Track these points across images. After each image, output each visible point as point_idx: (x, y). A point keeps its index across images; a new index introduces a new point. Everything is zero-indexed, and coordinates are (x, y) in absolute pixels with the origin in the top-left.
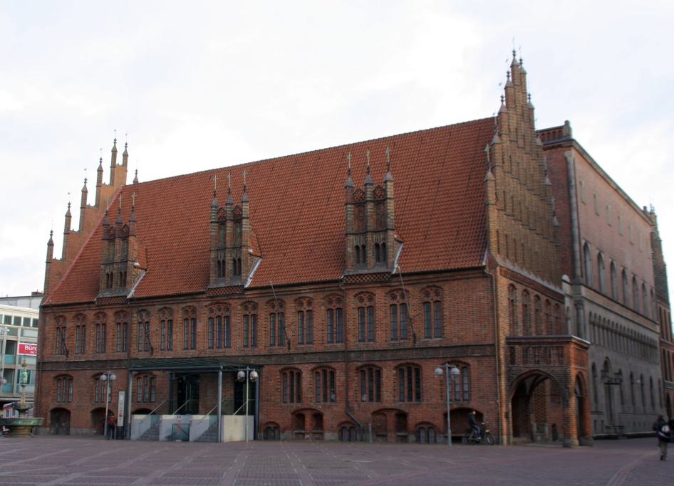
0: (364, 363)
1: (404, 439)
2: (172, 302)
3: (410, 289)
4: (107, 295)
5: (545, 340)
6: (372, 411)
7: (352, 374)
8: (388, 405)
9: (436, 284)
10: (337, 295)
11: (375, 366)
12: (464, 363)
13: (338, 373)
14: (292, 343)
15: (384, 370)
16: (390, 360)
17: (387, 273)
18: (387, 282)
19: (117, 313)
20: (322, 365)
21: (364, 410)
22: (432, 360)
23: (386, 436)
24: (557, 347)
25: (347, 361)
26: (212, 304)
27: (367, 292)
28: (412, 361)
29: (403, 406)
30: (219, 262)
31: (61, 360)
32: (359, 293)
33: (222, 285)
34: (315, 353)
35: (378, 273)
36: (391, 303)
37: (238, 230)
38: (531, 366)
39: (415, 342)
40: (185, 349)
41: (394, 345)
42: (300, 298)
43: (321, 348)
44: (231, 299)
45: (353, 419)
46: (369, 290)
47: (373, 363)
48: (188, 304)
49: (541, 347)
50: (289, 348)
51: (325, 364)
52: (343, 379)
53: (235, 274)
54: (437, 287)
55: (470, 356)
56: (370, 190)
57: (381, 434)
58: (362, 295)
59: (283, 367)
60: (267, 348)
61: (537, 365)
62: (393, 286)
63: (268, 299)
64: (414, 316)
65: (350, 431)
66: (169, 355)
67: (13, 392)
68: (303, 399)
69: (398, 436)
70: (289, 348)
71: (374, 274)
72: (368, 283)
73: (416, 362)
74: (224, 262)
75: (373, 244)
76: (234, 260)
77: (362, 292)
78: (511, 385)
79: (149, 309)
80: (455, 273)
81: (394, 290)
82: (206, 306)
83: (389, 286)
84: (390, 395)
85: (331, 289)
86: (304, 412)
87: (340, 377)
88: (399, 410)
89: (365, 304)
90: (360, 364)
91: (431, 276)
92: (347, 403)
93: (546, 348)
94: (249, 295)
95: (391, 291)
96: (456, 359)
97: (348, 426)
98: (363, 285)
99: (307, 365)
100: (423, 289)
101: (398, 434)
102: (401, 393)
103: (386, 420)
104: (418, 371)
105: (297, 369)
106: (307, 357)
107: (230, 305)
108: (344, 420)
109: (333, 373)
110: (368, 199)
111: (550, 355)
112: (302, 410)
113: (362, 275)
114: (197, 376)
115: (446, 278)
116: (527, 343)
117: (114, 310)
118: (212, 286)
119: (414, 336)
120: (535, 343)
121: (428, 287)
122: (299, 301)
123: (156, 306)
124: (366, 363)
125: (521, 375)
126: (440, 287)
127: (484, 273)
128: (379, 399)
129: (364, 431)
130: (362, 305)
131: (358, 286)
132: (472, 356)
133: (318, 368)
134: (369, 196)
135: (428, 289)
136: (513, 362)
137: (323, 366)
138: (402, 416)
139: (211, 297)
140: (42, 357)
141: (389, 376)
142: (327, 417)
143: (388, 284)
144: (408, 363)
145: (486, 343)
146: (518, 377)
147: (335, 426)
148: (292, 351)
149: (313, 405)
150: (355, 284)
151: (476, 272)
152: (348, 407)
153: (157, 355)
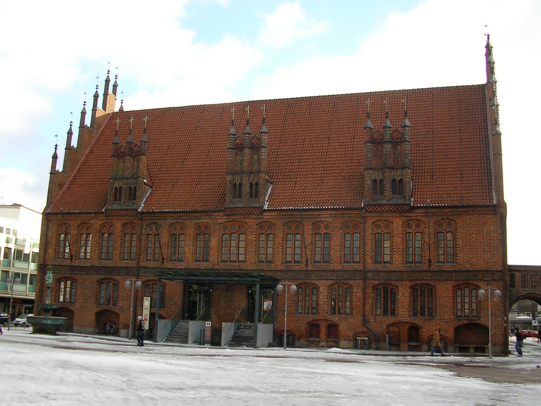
0: (381, 282)
2: (185, 218)
4: (116, 206)
6: (388, 323)
7: (369, 290)
14: (309, 262)
15: (400, 288)
16: (406, 280)
18: (406, 212)
19: (125, 225)
22: (445, 282)
25: (365, 279)
26: (227, 222)
27: (385, 220)
30: (235, 184)
31: (65, 263)
32: (377, 221)
33: (240, 205)
34: (333, 271)
35: (398, 205)
37: (256, 157)
39: (430, 266)
40: (196, 261)
42: (318, 222)
43: (339, 267)
44: (247, 218)
45: (369, 330)
46: (388, 219)
47: (390, 282)
48: (203, 221)
50: (307, 266)
52: (360, 295)
53: (251, 196)
54: (451, 219)
56: (389, 132)
58: (379, 223)
59: (300, 282)
60: (284, 264)
63: (286, 221)
66: (181, 265)
67: (7, 290)
68: (320, 311)
69: (409, 345)
70: (307, 266)
71: (393, 205)
73: (430, 283)
74: (240, 185)
76: (251, 184)
79: (160, 222)
82: (221, 223)
84: (403, 310)
90: (377, 282)
94: (267, 216)
95: (408, 221)
99: (325, 282)
101: (411, 344)
103: (399, 332)
104: (432, 289)
107: (246, 223)
108: (359, 331)
112: (317, 320)
113: (381, 205)
114: (211, 284)
117: (123, 222)
118: (228, 204)
119: (430, 261)
122: (316, 225)
123: (169, 221)
126: (453, 220)
128: (393, 313)
131: (377, 215)
132: (483, 280)
133: (335, 284)
135: (442, 221)
139: (228, 216)
140: (45, 259)
141: (403, 296)
142: (343, 328)
145: (495, 269)
148: (310, 268)
149: (330, 317)
150: (375, 211)
151: (488, 209)
152: (365, 321)
153: (169, 265)
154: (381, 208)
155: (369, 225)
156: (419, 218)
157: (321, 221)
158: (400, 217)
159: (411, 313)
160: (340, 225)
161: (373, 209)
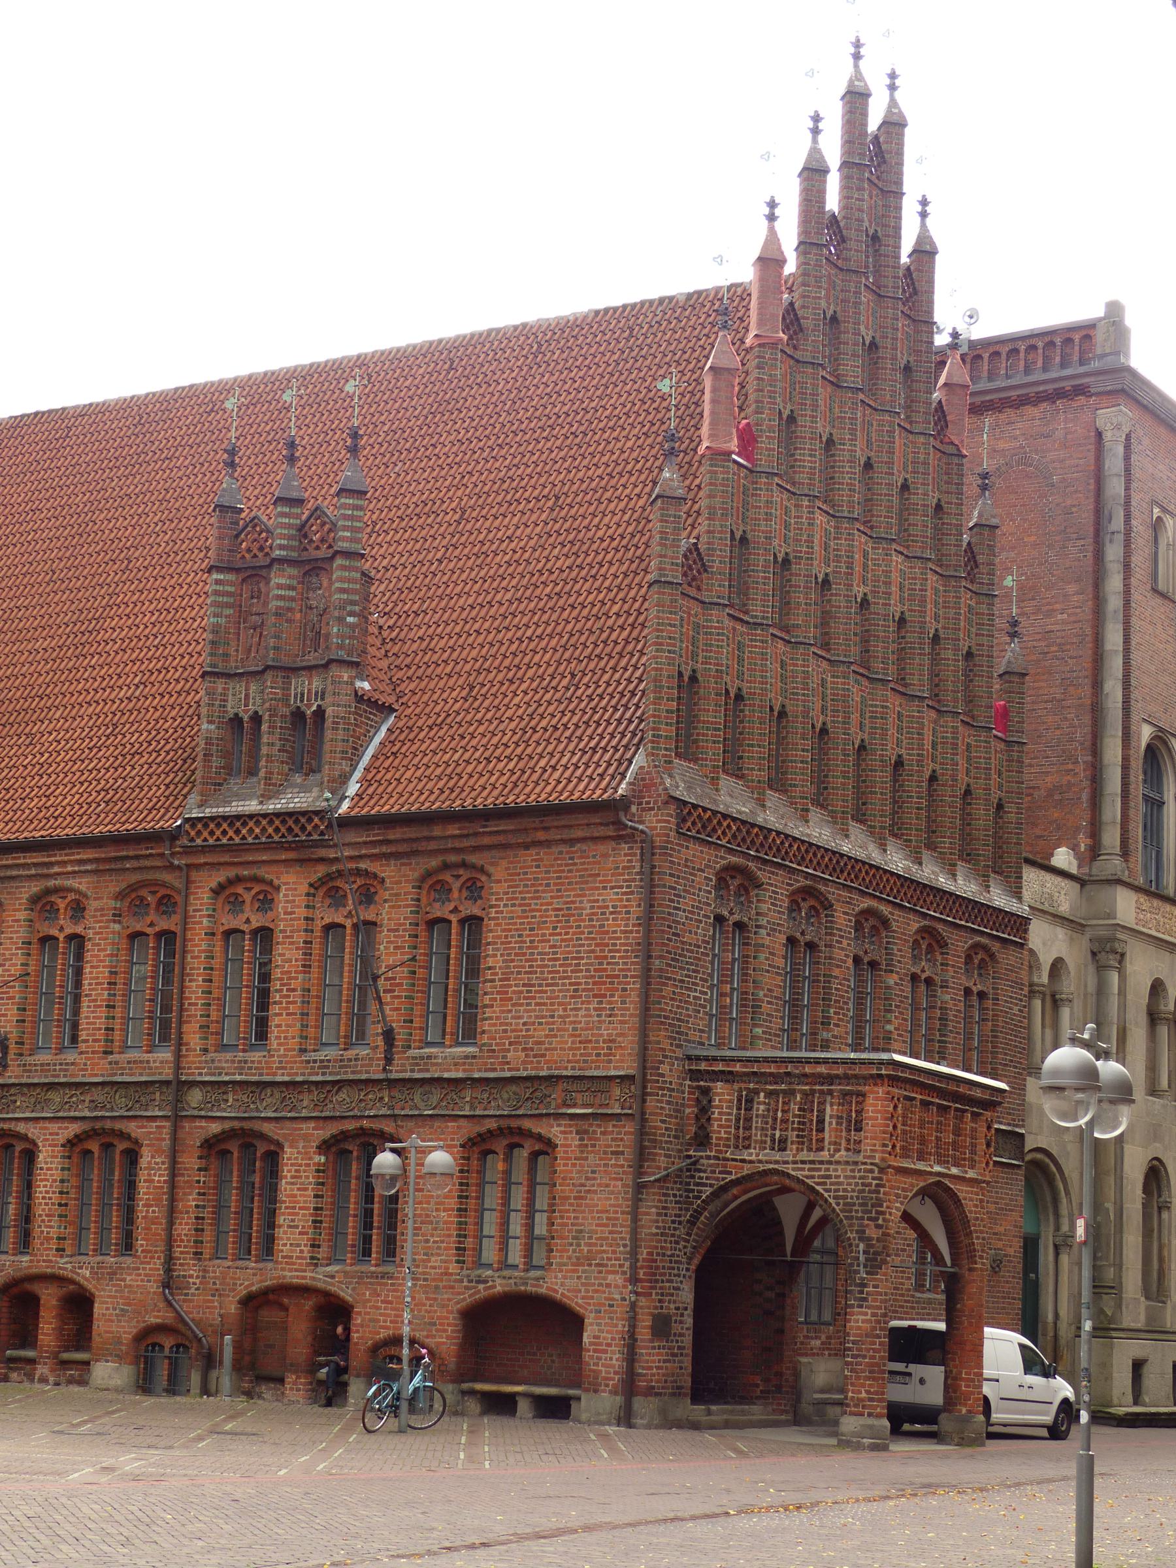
0: (227, 1125)
1: (331, 1393)
3: (387, 871)
5: (808, 1069)
7: (190, 1161)
8: (291, 1276)
9: (473, 859)
10: (164, 885)
11: (262, 1136)
12: (539, 1138)
13: (145, 1159)
17: (316, 813)
20: (98, 1125)
21: (216, 1290)
23: (281, 1381)
24: (845, 1094)
28: (376, 1125)
29: (333, 1277)
32: (231, 882)
35: (290, 814)
36: (327, 920)
38: (759, 1156)
39: (389, 1060)
41: (324, 1065)
42: (48, 892)
46: (262, 872)
49: (792, 1093)
51: (108, 1125)
52: (161, 1177)
55: (558, 1116)
57: (258, 1373)
61: (778, 1156)
62: (337, 860)
64: (391, 968)
65: (168, 1362)
72: (258, 847)
75: (286, 711)
77: (239, 879)
78: (692, 1223)
80: (526, 822)
81: (340, 873)
83: (322, 860)
85: (147, 863)
86: (36, 1288)
87: (152, 1170)
88: (327, 1294)
89: (248, 921)
90: (215, 1128)
91: (453, 830)
92: (169, 1260)
93: (805, 1094)
95: (329, 877)
96: (514, 1123)
97: (168, 1342)
98: (244, 854)
99: (54, 1127)
100: (429, 874)
102: (337, 1234)
105: (24, 1138)
106: (55, 1097)
109: (132, 1156)
110: (277, 553)
111: (821, 1121)
115: (501, 839)
116: (753, 1079)
119: (389, 1036)
120: (776, 1078)
121: (446, 866)
124: (236, 1124)
125: (724, 1189)
127: (618, 824)
129: (210, 1361)
130: (236, 922)
134: (280, 545)
136: (702, 1139)
137: (103, 1132)
138: (334, 1312)
143: (322, 853)
144: (362, 1132)
146: (715, 1195)
147: (127, 1338)
149: (64, 1265)
152: (169, 1282)
154: (237, 832)
155: (201, 899)
156: (363, 865)
157: (56, 890)
158: (301, 861)
159: (323, 1253)
160: (112, 903)
161: (212, 833)
